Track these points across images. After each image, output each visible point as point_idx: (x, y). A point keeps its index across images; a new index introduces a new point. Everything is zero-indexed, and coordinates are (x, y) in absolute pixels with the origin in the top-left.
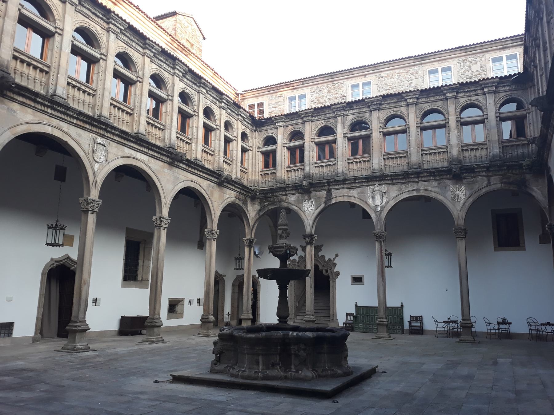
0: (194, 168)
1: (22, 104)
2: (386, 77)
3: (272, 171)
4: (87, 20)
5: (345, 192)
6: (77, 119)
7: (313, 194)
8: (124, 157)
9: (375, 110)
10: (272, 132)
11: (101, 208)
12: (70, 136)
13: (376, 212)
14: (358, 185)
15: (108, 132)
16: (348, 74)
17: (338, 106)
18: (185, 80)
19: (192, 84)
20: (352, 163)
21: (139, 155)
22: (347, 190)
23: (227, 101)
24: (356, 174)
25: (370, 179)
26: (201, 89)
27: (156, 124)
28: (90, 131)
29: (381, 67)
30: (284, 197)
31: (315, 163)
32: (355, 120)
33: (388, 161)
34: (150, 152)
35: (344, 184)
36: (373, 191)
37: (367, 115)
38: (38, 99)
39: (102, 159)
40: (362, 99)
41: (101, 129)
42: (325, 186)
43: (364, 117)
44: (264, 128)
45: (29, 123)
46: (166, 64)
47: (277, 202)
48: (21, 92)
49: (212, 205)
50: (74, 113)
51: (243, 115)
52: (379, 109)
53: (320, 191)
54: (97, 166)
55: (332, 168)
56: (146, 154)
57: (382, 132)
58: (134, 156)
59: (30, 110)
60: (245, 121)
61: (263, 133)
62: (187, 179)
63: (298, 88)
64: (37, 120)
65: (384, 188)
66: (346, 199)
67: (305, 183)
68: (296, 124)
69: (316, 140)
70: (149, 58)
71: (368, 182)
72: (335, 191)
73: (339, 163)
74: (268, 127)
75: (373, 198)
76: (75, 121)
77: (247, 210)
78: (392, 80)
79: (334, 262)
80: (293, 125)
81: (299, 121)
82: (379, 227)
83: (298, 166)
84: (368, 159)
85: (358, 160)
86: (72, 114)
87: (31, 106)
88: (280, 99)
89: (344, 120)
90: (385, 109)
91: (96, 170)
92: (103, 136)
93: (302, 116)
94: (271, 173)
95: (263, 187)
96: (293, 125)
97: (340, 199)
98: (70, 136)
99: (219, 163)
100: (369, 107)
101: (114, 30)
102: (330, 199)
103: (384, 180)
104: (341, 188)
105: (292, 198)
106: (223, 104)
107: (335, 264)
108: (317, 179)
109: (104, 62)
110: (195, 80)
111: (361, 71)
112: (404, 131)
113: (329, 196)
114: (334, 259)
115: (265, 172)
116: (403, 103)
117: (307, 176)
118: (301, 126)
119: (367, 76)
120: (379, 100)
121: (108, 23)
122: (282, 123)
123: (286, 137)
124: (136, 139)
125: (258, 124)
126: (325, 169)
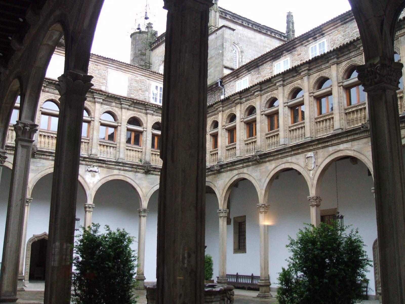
1: (269, 161)
4: (293, 84)
8: (330, 155)
21: (342, 147)
45: (274, 169)
56: (347, 142)
59: (273, 162)
70: (335, 64)
76: (293, 153)
101: (304, 74)
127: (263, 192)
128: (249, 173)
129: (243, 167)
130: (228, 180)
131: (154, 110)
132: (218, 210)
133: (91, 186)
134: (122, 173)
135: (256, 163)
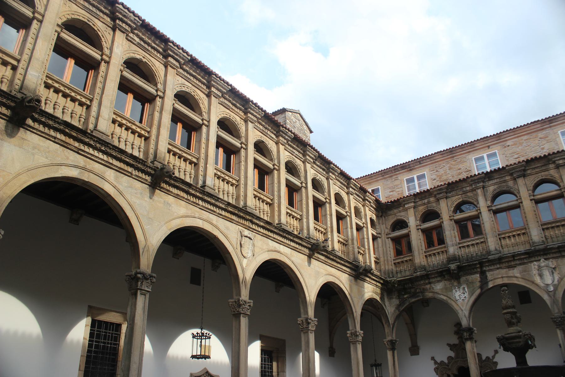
0: (333, 260)
1: (177, 196)
2: (512, 145)
3: (408, 258)
4: (228, 111)
5: (503, 272)
6: (225, 210)
7: (463, 279)
9: (519, 177)
10: (401, 215)
11: (253, 309)
12: (219, 229)
13: (548, 292)
14: (518, 262)
15: (253, 223)
16: (469, 147)
17: (476, 178)
18: (315, 166)
19: (321, 170)
20: (504, 238)
21: (282, 248)
22: (505, 270)
23: (355, 185)
24: (512, 250)
25: (534, 253)
26: (331, 174)
27: (293, 214)
28: (237, 223)
29: (505, 136)
30: (428, 286)
31: (459, 244)
32: (498, 191)
33: (548, 231)
34: (292, 244)
35: (500, 263)
36: (540, 268)
37: (511, 183)
38: (191, 190)
39: (250, 254)
40: (503, 167)
41: (247, 220)
42: (476, 268)
43: (508, 186)
44: (392, 212)
46: (298, 151)
47: (419, 292)
49: (353, 301)
51: (369, 200)
52: (524, 176)
53: (471, 274)
54: (245, 262)
55: (480, 247)
57: (534, 199)
58: (278, 249)
60: (371, 206)
61: (391, 217)
62: (327, 273)
63: (414, 169)
64: (189, 213)
65: (552, 263)
66: (506, 281)
67: (453, 266)
68: (429, 202)
69: (455, 218)
71: (530, 257)
72: (491, 273)
73: (489, 240)
74: (395, 211)
75: (541, 276)
76: (223, 213)
77: (385, 306)
78: (520, 148)
79: (495, 360)
80: (424, 204)
81: (432, 199)
82: (556, 311)
83: (438, 249)
84: (523, 231)
85: (511, 234)
86: (221, 205)
87: (184, 198)
88: (397, 182)
89: (484, 192)
90: (530, 174)
91: (244, 266)
92: (248, 228)
93: (435, 193)
94: (406, 261)
95: (399, 277)
96: (424, 204)
97: (499, 282)
98: (219, 229)
99: (354, 254)
100: (511, 175)
102: (487, 283)
103: (549, 254)
104: (498, 269)
105: (438, 287)
106: (351, 189)
107: (496, 363)
108: (465, 262)
110: (323, 165)
111: (483, 143)
112: (517, 206)
113: (484, 281)
114: (494, 357)
115: (399, 260)
116: (552, 166)
117: (453, 259)
118: (434, 205)
119: (491, 147)
120: (522, 166)
121: (246, 113)
122: (412, 204)
123: (418, 219)
124: (280, 230)
125: (382, 209)
126: (472, 249)
128: (121, 188)
129: (109, 166)
130: (42, 160)
135: (146, 180)
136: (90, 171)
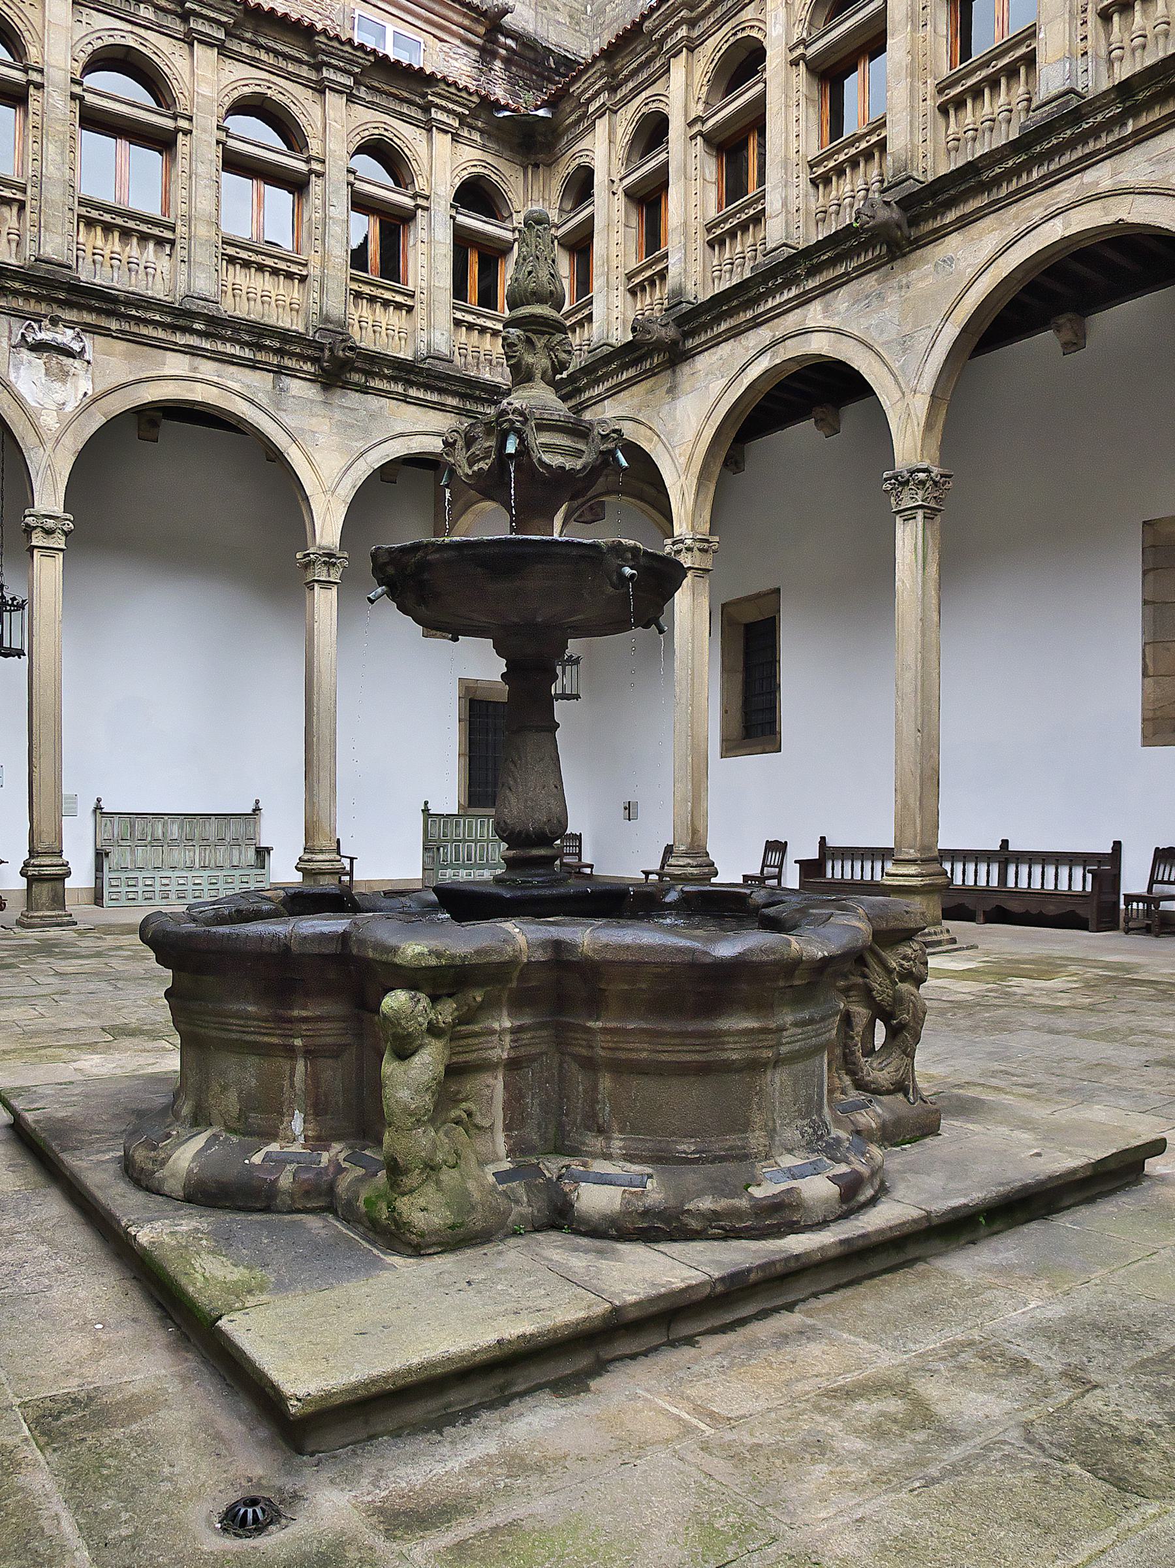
1: (964, 223)
48: (941, 198)
50: (1107, 106)
109: (425, 214)
127: (921, 404)
129: (804, 300)
130: (718, 385)
131: (357, 70)
132: (669, 541)
133: (49, 421)
134: (208, 369)
135: (879, 257)
136: (785, 339)
